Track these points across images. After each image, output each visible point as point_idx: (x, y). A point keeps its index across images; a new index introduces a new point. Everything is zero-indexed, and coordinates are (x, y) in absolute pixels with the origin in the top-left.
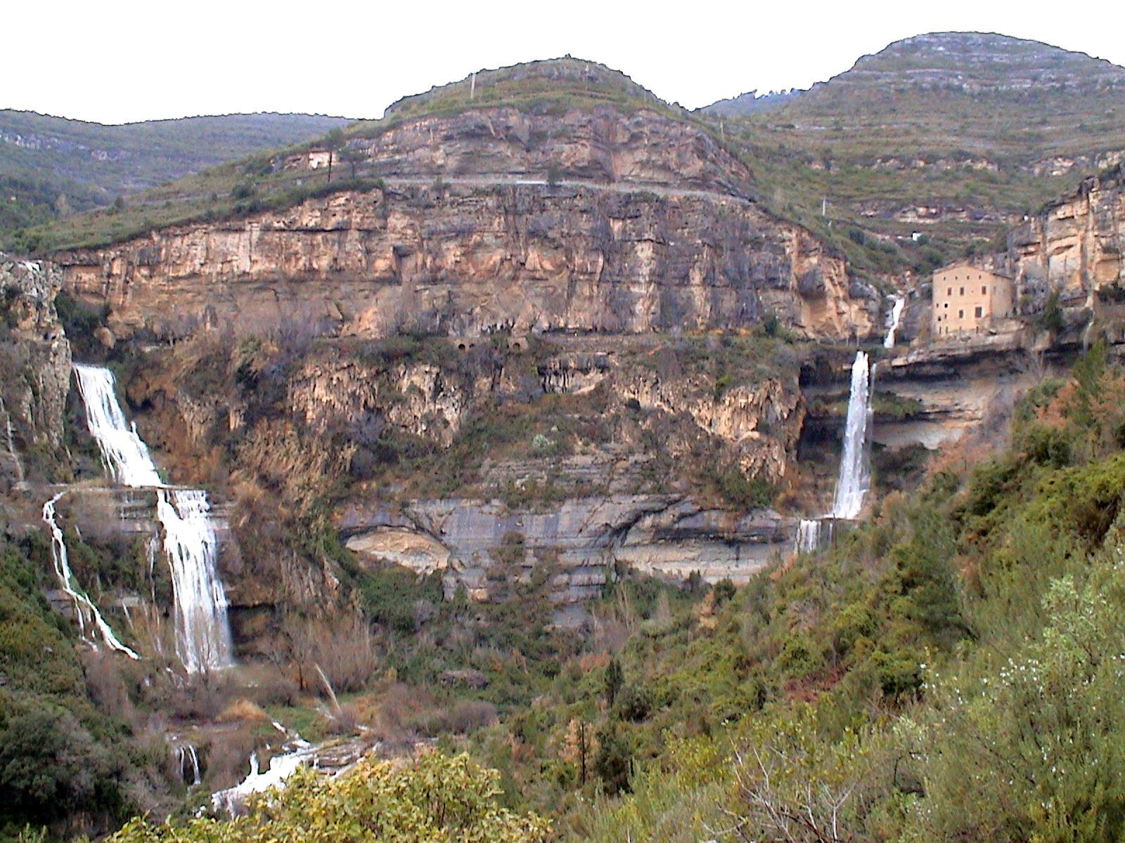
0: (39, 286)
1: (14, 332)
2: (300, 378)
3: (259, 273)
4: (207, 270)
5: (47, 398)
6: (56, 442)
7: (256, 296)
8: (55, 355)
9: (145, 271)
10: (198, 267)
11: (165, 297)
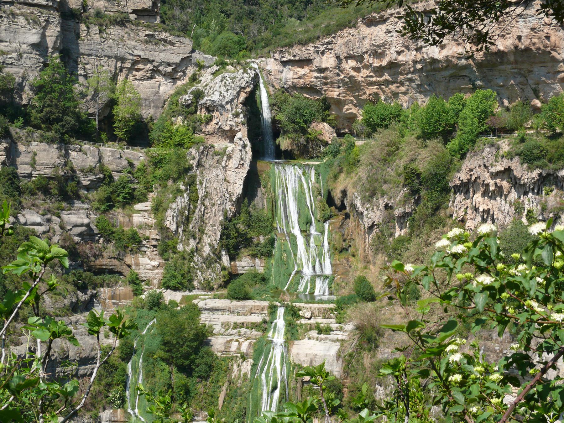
0: (223, 89)
1: (198, 136)
2: (458, 183)
3: (447, 59)
4: (401, 58)
5: (207, 202)
6: (207, 250)
7: (452, 85)
8: (230, 157)
9: (352, 63)
10: (394, 56)
11: (374, 89)
